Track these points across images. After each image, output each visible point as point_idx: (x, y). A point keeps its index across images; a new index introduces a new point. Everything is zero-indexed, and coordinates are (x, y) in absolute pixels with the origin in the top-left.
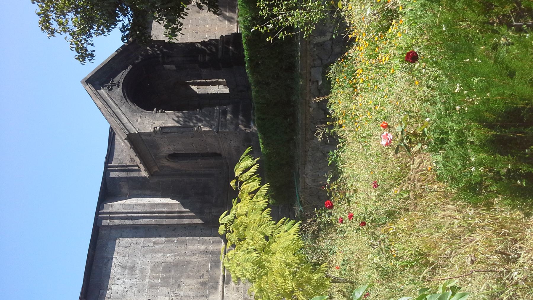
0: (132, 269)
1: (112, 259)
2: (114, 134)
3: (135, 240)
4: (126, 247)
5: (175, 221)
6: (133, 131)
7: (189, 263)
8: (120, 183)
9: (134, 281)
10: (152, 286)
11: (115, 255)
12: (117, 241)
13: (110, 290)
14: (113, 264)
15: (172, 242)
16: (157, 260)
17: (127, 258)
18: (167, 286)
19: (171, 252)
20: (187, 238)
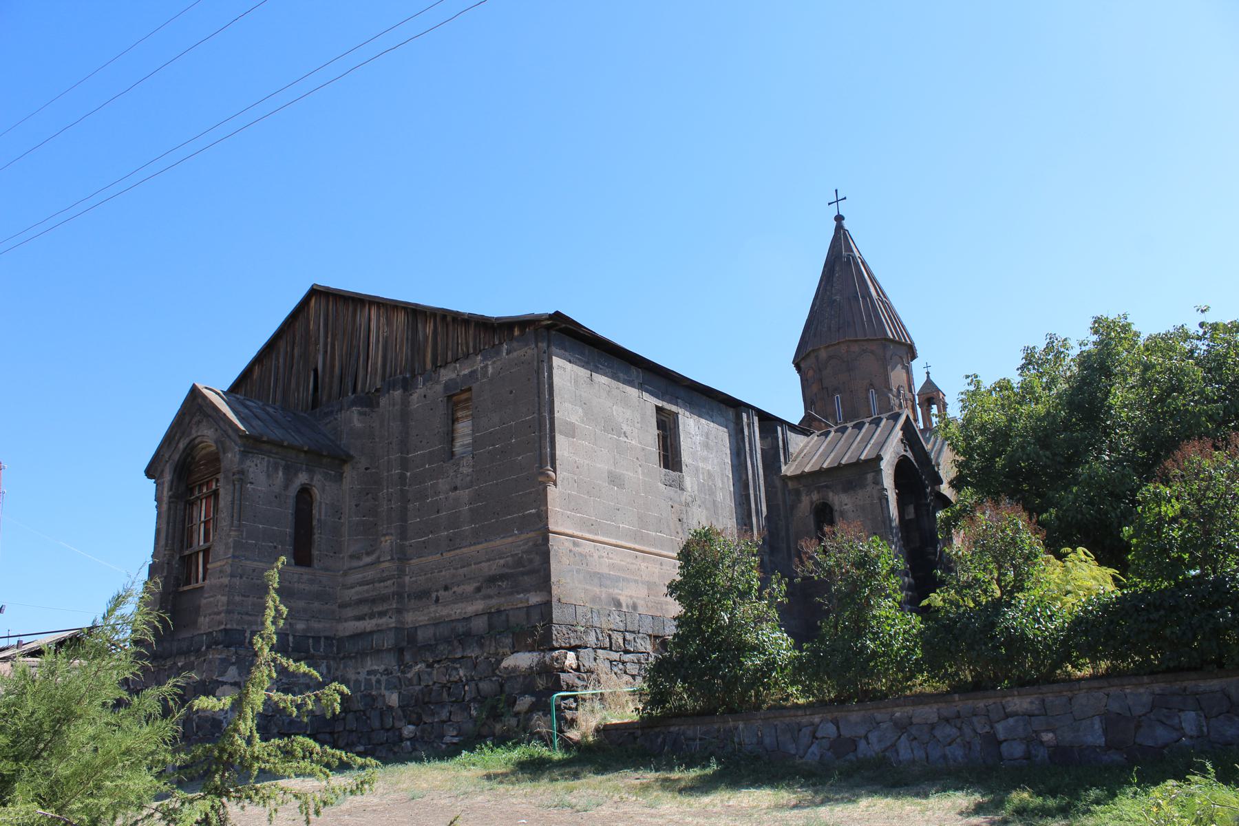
0: (706, 446)
2: (808, 436)
3: (729, 452)
6: (883, 465)
7: (718, 520)
8: (770, 438)
10: (697, 469)
12: (725, 430)
19: (724, 499)
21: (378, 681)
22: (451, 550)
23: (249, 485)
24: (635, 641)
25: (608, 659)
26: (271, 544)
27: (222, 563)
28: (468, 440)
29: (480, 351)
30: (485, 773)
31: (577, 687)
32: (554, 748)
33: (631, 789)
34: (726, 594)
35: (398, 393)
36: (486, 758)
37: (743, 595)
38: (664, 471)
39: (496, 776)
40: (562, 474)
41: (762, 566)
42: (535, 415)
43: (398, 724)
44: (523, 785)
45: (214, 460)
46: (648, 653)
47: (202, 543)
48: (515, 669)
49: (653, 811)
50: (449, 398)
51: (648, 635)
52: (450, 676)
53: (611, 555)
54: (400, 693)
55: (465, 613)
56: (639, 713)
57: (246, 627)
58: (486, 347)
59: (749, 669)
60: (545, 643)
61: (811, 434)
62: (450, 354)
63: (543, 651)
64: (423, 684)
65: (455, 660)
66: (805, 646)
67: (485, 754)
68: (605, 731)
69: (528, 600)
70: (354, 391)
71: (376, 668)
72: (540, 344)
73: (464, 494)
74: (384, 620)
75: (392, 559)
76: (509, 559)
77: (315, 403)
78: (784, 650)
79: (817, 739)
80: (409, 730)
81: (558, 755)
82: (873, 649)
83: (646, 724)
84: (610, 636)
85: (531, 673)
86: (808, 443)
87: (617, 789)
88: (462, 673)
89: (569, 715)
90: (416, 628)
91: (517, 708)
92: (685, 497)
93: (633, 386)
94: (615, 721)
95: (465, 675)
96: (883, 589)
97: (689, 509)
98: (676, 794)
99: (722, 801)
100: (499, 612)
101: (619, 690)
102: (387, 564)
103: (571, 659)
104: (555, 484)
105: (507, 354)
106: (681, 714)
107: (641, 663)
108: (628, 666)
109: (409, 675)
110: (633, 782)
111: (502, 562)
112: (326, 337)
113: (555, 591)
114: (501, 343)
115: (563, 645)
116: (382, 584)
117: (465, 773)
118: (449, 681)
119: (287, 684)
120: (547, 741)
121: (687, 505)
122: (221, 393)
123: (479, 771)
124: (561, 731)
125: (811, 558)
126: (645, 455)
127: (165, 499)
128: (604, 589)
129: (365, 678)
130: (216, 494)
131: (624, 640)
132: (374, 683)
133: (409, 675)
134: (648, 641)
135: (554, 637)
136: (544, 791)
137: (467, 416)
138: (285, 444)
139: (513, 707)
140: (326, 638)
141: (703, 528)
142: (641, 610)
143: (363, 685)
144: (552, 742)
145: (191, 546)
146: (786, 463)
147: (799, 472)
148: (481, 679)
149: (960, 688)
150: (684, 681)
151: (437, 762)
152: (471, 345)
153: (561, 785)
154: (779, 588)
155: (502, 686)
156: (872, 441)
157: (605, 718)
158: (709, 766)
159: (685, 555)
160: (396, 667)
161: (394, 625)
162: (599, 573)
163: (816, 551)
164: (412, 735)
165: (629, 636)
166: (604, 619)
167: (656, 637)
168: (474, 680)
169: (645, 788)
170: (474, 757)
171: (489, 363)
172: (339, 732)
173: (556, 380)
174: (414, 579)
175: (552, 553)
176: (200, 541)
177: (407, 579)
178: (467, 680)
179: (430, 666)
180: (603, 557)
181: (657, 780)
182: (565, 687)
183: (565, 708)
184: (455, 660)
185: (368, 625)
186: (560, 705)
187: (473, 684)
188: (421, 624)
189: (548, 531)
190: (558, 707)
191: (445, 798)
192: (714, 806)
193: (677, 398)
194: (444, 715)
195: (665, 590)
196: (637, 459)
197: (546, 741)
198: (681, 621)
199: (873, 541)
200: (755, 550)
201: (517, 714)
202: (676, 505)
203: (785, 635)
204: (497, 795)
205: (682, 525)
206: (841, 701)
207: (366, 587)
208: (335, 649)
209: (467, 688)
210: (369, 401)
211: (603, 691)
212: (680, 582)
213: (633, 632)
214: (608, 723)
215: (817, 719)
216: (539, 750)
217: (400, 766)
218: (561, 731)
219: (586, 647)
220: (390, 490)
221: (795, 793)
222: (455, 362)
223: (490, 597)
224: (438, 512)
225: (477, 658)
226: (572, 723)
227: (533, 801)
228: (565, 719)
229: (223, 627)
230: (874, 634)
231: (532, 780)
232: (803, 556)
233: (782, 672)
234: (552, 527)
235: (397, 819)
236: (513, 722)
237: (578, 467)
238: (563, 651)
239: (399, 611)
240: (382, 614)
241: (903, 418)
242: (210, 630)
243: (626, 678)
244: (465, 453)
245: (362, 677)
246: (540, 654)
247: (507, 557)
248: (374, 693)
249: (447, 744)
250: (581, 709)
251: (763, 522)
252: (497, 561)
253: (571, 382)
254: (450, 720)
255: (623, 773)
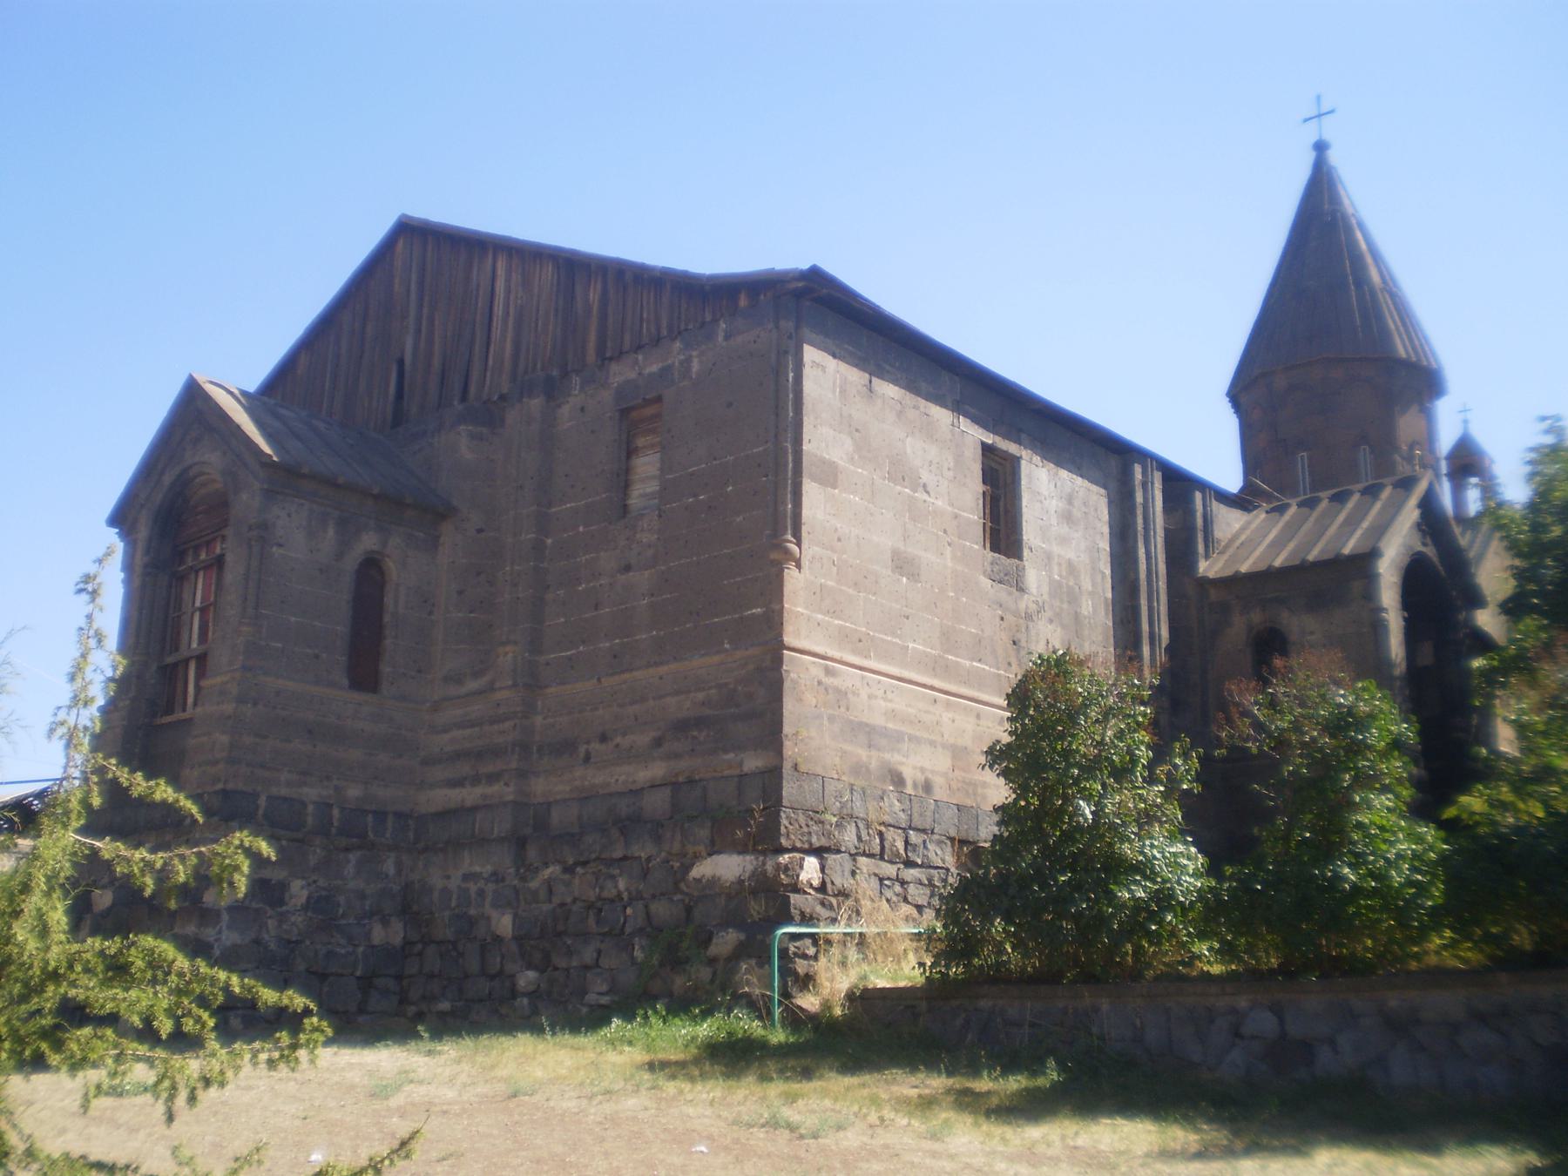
0: (1067, 518)
1: (1081, 476)
3: (1106, 530)
4: (1096, 510)
5: (1145, 627)
9: (1054, 521)
11: (1086, 483)
12: (1103, 491)
13: (1041, 464)
14: (1075, 476)
15: (1107, 614)
16: (1082, 577)
17: (1084, 509)
18: (1050, 594)
20: (1112, 649)
21: (481, 893)
22: (613, 674)
23: (274, 549)
24: (925, 847)
25: (876, 875)
26: (309, 651)
27: (225, 678)
28: (653, 487)
29: (680, 333)
30: (647, 1058)
31: (818, 920)
32: (773, 1025)
33: (903, 1104)
34: (1091, 768)
35: (536, 404)
36: (653, 1034)
37: (1122, 773)
38: (990, 555)
39: (664, 1065)
40: (810, 550)
41: (1154, 726)
42: (769, 444)
43: (510, 967)
44: (710, 1084)
45: (220, 506)
46: (948, 870)
47: (194, 645)
48: (714, 881)
49: (937, 1146)
50: (624, 412)
51: (952, 839)
52: (602, 888)
53: (889, 695)
54: (515, 916)
55: (634, 782)
56: (924, 969)
57: (259, 788)
58: (691, 326)
59: (1124, 905)
60: (766, 840)
61: (1256, 508)
62: (627, 338)
63: (764, 853)
64: (556, 900)
65: (611, 862)
66: (1229, 870)
67: (651, 1027)
68: (862, 998)
69: (741, 764)
70: (464, 398)
71: (477, 869)
72: (783, 323)
73: (642, 579)
74: (496, 788)
75: (515, 685)
76: (713, 691)
77: (398, 418)
78: (1191, 876)
79: (1242, 1037)
80: (527, 978)
81: (778, 1036)
82: (1354, 883)
83: (935, 991)
84: (881, 834)
85: (740, 891)
86: (1249, 523)
87: (875, 1101)
88: (622, 884)
89: (801, 966)
90: (549, 804)
91: (713, 950)
92: (1026, 602)
93: (943, 405)
94: (882, 983)
95: (627, 889)
96: (1377, 777)
97: (1031, 625)
98: (982, 1119)
99: (1063, 1138)
100: (691, 782)
101: (892, 929)
102: (504, 694)
103: (810, 870)
104: (799, 566)
105: (727, 338)
106: (998, 977)
107: (934, 886)
108: (912, 889)
109: (534, 884)
110: (905, 1092)
111: (701, 696)
112: (420, 307)
113: (790, 750)
114: (715, 321)
115: (798, 845)
116: (496, 727)
117: (612, 1057)
118: (599, 898)
119: (324, 889)
120: (760, 1009)
121: (1029, 617)
122: (236, 392)
123: (637, 1055)
124: (786, 995)
125: (1246, 713)
126: (958, 527)
127: (138, 569)
128: (874, 753)
129: (459, 887)
130: (220, 562)
131: (907, 842)
132: (473, 896)
133: (534, 884)
134: (949, 849)
135: (782, 828)
136: (746, 1098)
137: (653, 446)
138: (341, 480)
139: (706, 948)
140: (399, 815)
141: (1054, 652)
142: (940, 793)
143: (455, 896)
144: (770, 1013)
145: (177, 649)
146: (1207, 557)
147: (1228, 572)
148: (654, 896)
149: (1510, 962)
150: (1008, 920)
151: (566, 1036)
152: (664, 323)
153: (776, 1088)
154: (1185, 766)
155: (689, 910)
156: (1365, 524)
157: (864, 978)
158: (1044, 1074)
159: (1019, 698)
160: (512, 870)
161: (510, 798)
162: (867, 725)
163: (1256, 703)
164: (532, 988)
165: (914, 837)
166: (872, 805)
167: (963, 842)
168: (642, 898)
169: (926, 1104)
170: (632, 1029)
171: (695, 353)
172: (411, 976)
173: (809, 386)
174: (551, 720)
175: (787, 685)
176: (192, 642)
177: (538, 720)
178: (630, 899)
179: (569, 870)
180: (876, 697)
181: (948, 1091)
182: (797, 918)
183: (795, 954)
184: (611, 862)
185: (469, 795)
186: (787, 949)
187: (640, 905)
188: (558, 797)
189: (781, 646)
190: (784, 953)
191: (570, 1099)
192: (1049, 1145)
193: (1020, 430)
194: (588, 955)
195: (983, 760)
196: (945, 532)
197: (759, 1010)
198: (1006, 813)
199: (1364, 689)
200: (1147, 693)
201: (712, 961)
202: (1009, 618)
203: (1193, 850)
204: (661, 1099)
205: (1018, 651)
206: (1289, 972)
207: (468, 732)
208: (411, 835)
209: (629, 911)
210: (489, 416)
211: (864, 930)
212: (1009, 745)
213: (924, 831)
214: (871, 986)
215: (1243, 1002)
216: (747, 1024)
217: (503, 1039)
218: (786, 995)
219: (838, 851)
220: (517, 568)
221: (1197, 1130)
222: (636, 352)
223: (677, 756)
224: (596, 608)
225: (649, 859)
226: (807, 982)
227: (725, 1114)
228: (796, 974)
229: (220, 786)
230: (1357, 855)
231: (727, 1076)
232: (1233, 709)
233: (1184, 915)
234: (788, 639)
235: (480, 1129)
236: (705, 973)
237: (839, 540)
238: (798, 855)
239: (522, 774)
240: (492, 778)
241: (1422, 487)
242: (199, 791)
243: (907, 909)
244: (645, 508)
245: (455, 883)
246: (757, 859)
247: (710, 688)
248: (472, 912)
249: (591, 1006)
250: (823, 960)
251: (1162, 657)
252: (692, 695)
253: (834, 392)
254: (597, 965)
255: (890, 1074)
